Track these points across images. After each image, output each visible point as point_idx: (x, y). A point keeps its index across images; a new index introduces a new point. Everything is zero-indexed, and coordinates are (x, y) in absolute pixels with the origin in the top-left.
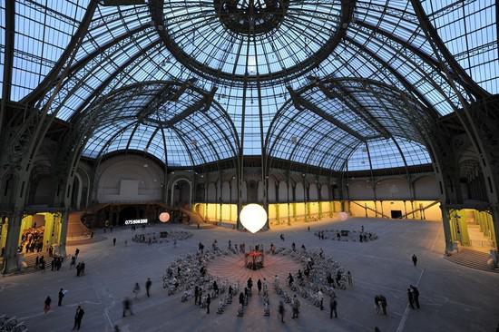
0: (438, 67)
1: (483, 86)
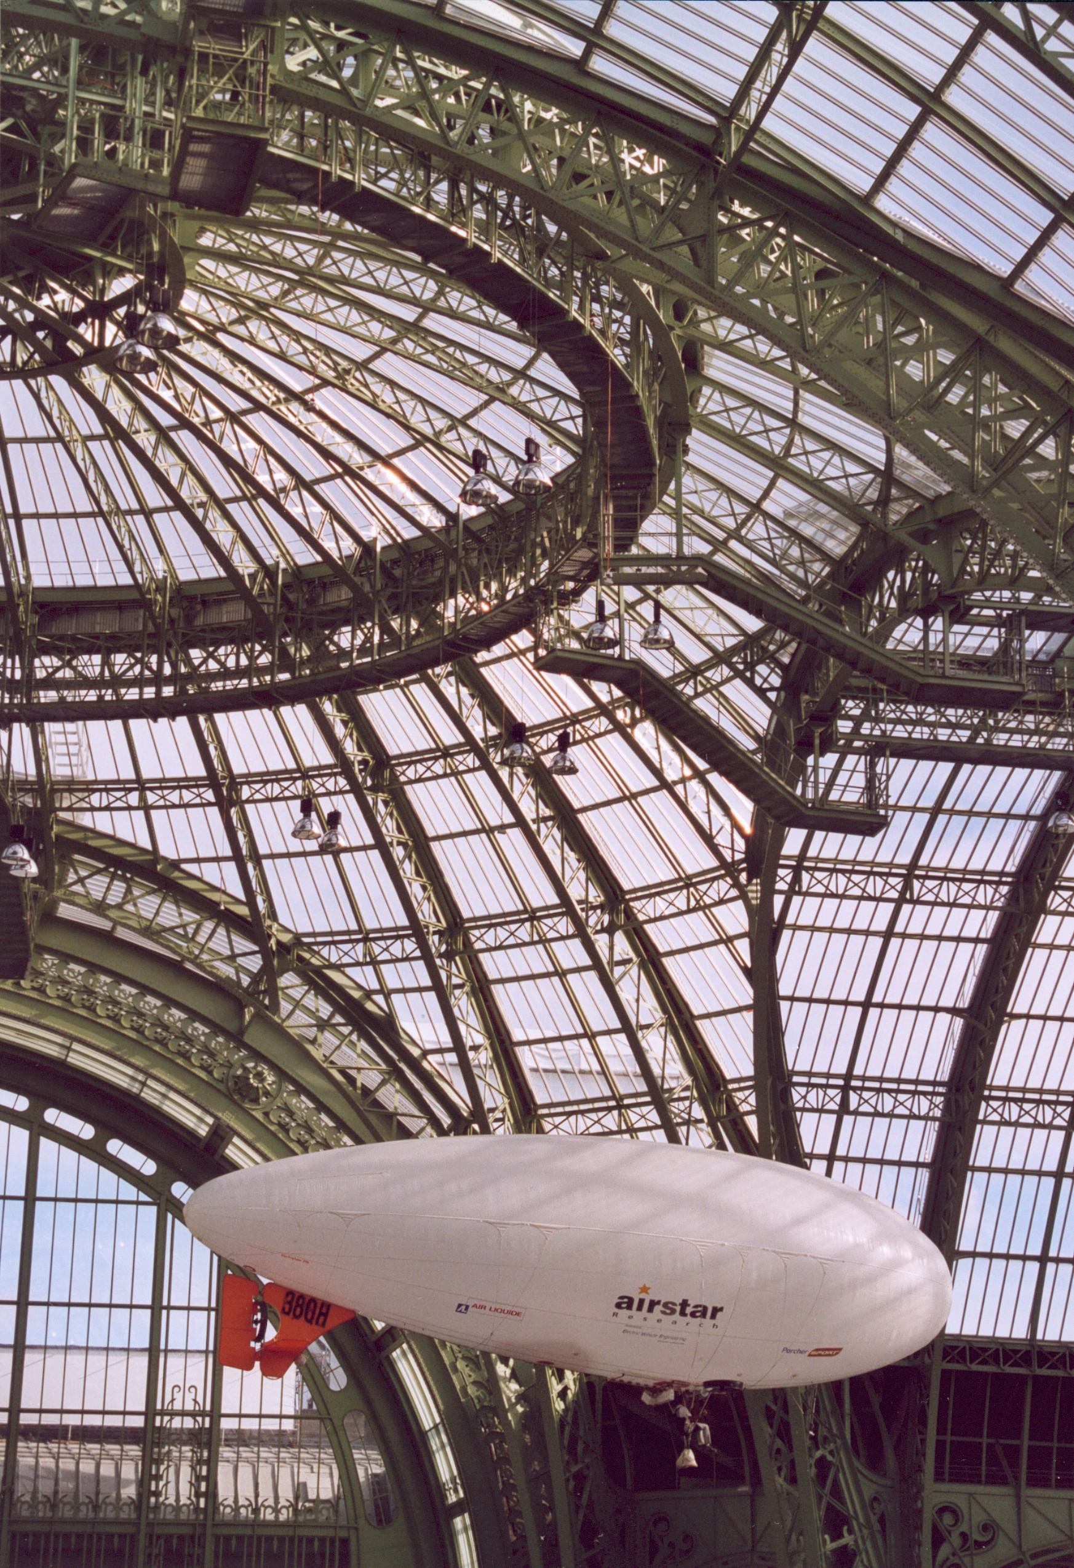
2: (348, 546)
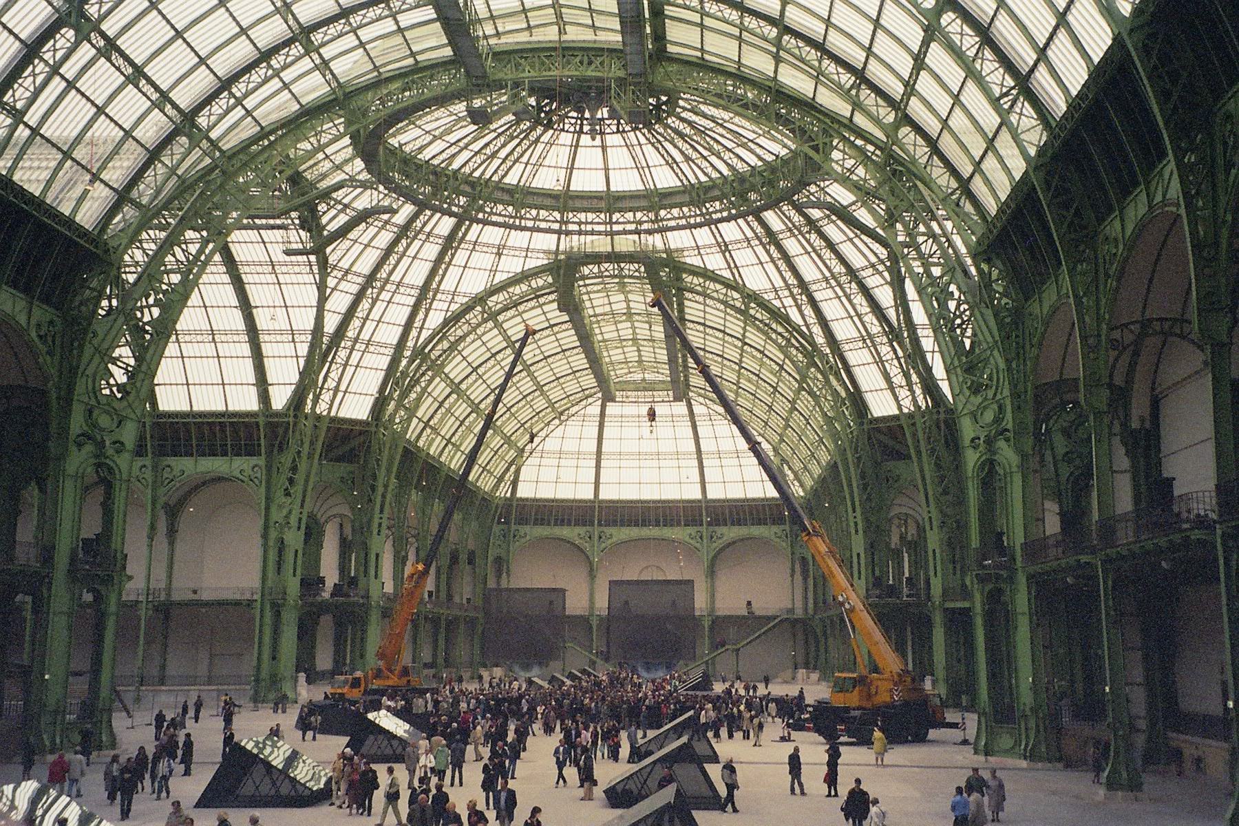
0: (893, 334)
2: (747, 168)
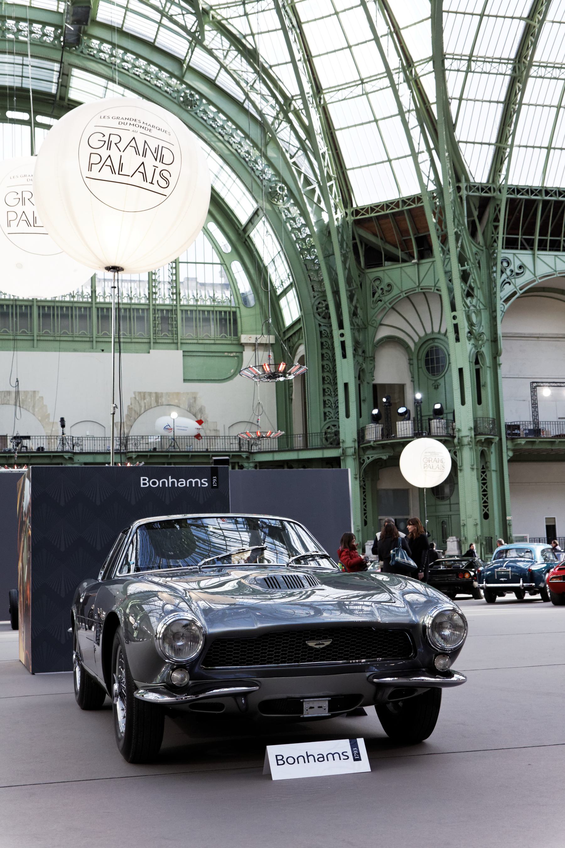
1: (466, 152)
